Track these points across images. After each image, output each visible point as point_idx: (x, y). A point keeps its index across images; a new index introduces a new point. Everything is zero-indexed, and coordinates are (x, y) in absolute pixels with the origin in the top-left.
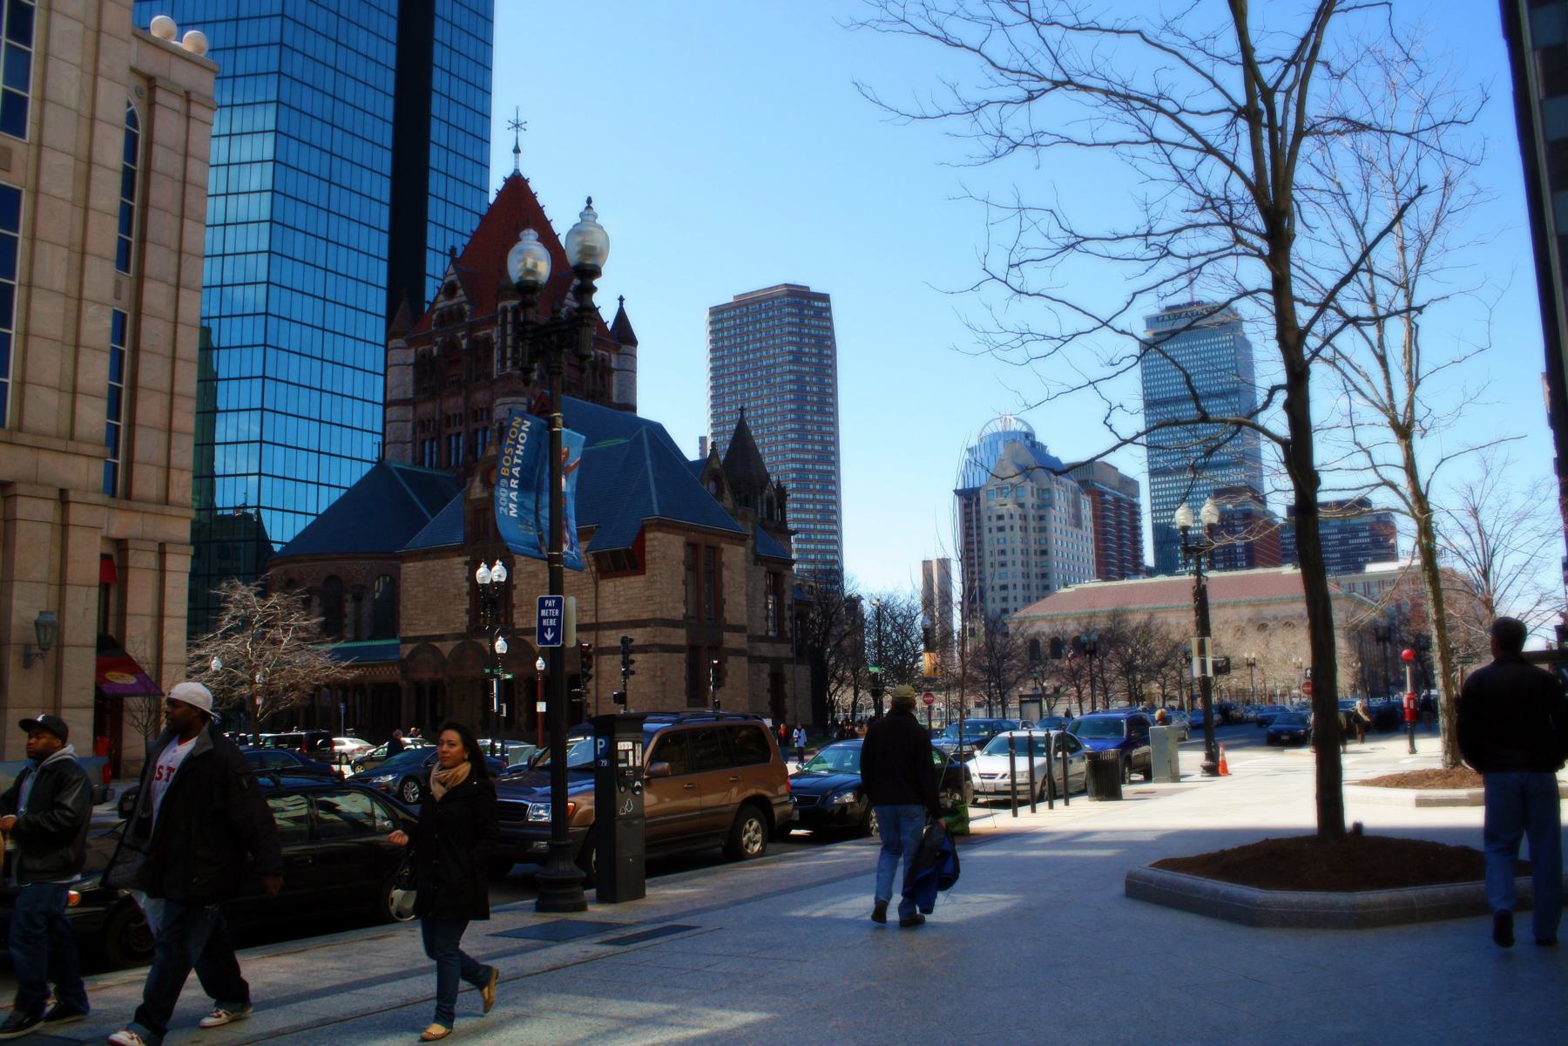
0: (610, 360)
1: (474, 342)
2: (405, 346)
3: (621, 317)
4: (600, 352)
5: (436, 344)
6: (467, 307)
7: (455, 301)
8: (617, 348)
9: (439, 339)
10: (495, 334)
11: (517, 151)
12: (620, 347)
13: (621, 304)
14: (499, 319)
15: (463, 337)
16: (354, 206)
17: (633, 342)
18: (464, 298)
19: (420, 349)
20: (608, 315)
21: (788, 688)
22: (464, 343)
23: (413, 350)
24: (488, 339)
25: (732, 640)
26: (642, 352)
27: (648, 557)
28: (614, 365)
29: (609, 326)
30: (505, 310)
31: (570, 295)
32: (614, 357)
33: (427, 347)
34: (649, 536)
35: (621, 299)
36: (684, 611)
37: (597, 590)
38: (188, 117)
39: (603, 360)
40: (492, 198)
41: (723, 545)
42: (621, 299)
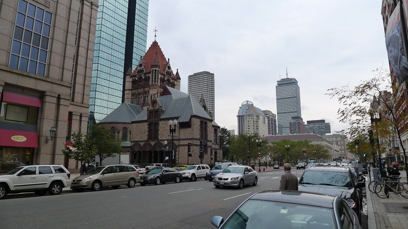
1: (146, 77)
2: (130, 77)
3: (177, 73)
5: (137, 77)
6: (144, 69)
7: (142, 68)
8: (176, 80)
10: (150, 75)
11: (155, 36)
13: (177, 71)
14: (152, 72)
16: (117, 48)
17: (180, 79)
18: (144, 67)
20: (175, 73)
21: (218, 155)
22: (143, 77)
24: (149, 77)
25: (209, 144)
26: (181, 81)
27: (192, 124)
33: (135, 78)
34: (192, 119)
35: (177, 69)
37: (179, 131)
38: (92, 8)
39: (173, 82)
40: (148, 49)
42: (177, 69)
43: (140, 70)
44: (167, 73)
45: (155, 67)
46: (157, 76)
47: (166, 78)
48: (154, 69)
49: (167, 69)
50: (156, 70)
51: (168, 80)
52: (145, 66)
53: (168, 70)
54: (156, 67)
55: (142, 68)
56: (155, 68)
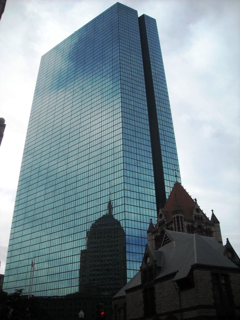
0: (211, 229)
4: (208, 227)
6: (165, 220)
7: (162, 219)
8: (213, 225)
9: (159, 231)
12: (214, 224)
13: (213, 212)
15: (165, 228)
17: (218, 223)
19: (156, 234)
20: (209, 216)
23: (154, 235)
28: (213, 230)
29: (210, 219)
30: (174, 218)
31: (195, 211)
32: (212, 228)
33: (157, 234)
34: (194, 272)
35: (212, 211)
36: (214, 301)
37: (180, 296)
39: (209, 229)
41: (230, 274)
42: (212, 211)
43: (161, 222)
44: (195, 217)
45: (176, 214)
46: (176, 224)
47: (195, 226)
48: (175, 216)
49: (195, 213)
50: (178, 217)
51: (200, 227)
52: (165, 216)
53: (197, 214)
54: (178, 213)
55: (162, 219)
56: (177, 215)
